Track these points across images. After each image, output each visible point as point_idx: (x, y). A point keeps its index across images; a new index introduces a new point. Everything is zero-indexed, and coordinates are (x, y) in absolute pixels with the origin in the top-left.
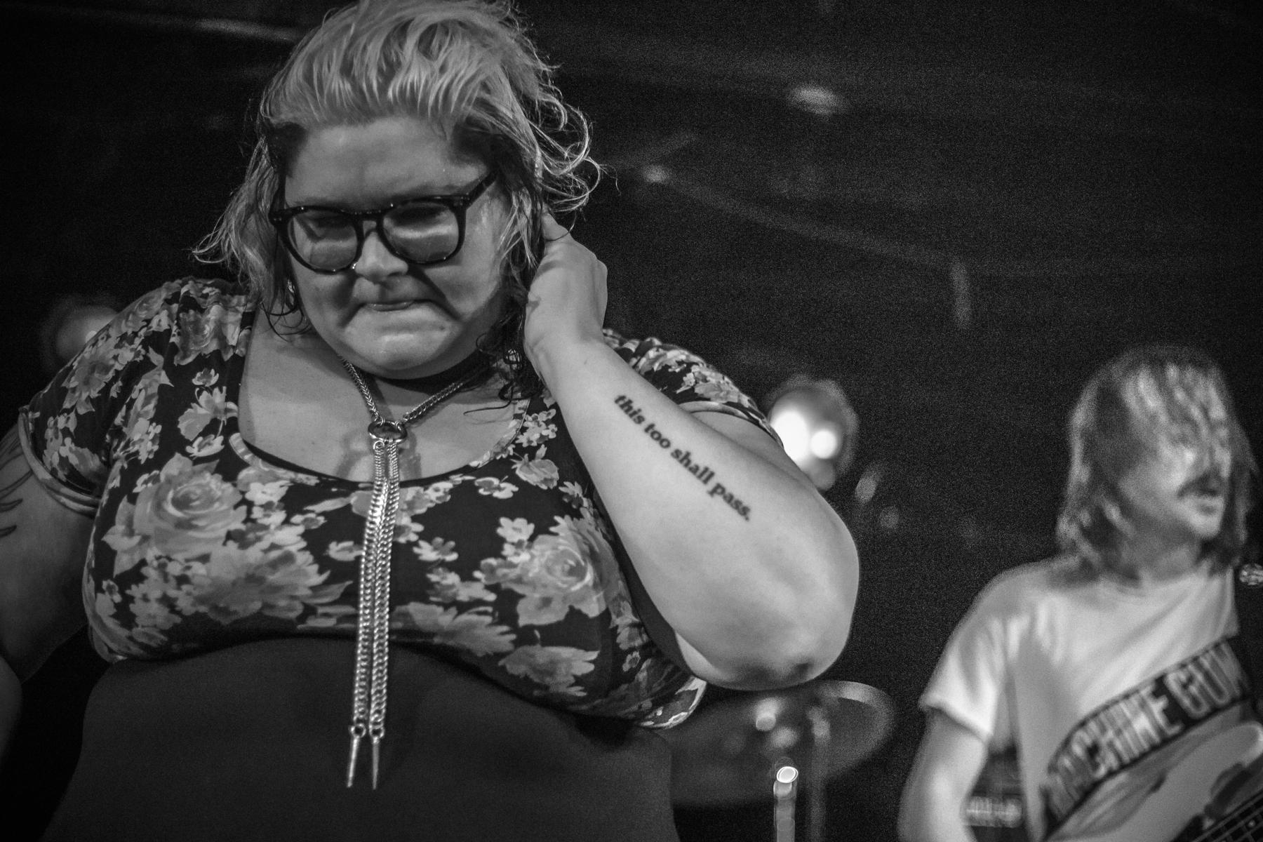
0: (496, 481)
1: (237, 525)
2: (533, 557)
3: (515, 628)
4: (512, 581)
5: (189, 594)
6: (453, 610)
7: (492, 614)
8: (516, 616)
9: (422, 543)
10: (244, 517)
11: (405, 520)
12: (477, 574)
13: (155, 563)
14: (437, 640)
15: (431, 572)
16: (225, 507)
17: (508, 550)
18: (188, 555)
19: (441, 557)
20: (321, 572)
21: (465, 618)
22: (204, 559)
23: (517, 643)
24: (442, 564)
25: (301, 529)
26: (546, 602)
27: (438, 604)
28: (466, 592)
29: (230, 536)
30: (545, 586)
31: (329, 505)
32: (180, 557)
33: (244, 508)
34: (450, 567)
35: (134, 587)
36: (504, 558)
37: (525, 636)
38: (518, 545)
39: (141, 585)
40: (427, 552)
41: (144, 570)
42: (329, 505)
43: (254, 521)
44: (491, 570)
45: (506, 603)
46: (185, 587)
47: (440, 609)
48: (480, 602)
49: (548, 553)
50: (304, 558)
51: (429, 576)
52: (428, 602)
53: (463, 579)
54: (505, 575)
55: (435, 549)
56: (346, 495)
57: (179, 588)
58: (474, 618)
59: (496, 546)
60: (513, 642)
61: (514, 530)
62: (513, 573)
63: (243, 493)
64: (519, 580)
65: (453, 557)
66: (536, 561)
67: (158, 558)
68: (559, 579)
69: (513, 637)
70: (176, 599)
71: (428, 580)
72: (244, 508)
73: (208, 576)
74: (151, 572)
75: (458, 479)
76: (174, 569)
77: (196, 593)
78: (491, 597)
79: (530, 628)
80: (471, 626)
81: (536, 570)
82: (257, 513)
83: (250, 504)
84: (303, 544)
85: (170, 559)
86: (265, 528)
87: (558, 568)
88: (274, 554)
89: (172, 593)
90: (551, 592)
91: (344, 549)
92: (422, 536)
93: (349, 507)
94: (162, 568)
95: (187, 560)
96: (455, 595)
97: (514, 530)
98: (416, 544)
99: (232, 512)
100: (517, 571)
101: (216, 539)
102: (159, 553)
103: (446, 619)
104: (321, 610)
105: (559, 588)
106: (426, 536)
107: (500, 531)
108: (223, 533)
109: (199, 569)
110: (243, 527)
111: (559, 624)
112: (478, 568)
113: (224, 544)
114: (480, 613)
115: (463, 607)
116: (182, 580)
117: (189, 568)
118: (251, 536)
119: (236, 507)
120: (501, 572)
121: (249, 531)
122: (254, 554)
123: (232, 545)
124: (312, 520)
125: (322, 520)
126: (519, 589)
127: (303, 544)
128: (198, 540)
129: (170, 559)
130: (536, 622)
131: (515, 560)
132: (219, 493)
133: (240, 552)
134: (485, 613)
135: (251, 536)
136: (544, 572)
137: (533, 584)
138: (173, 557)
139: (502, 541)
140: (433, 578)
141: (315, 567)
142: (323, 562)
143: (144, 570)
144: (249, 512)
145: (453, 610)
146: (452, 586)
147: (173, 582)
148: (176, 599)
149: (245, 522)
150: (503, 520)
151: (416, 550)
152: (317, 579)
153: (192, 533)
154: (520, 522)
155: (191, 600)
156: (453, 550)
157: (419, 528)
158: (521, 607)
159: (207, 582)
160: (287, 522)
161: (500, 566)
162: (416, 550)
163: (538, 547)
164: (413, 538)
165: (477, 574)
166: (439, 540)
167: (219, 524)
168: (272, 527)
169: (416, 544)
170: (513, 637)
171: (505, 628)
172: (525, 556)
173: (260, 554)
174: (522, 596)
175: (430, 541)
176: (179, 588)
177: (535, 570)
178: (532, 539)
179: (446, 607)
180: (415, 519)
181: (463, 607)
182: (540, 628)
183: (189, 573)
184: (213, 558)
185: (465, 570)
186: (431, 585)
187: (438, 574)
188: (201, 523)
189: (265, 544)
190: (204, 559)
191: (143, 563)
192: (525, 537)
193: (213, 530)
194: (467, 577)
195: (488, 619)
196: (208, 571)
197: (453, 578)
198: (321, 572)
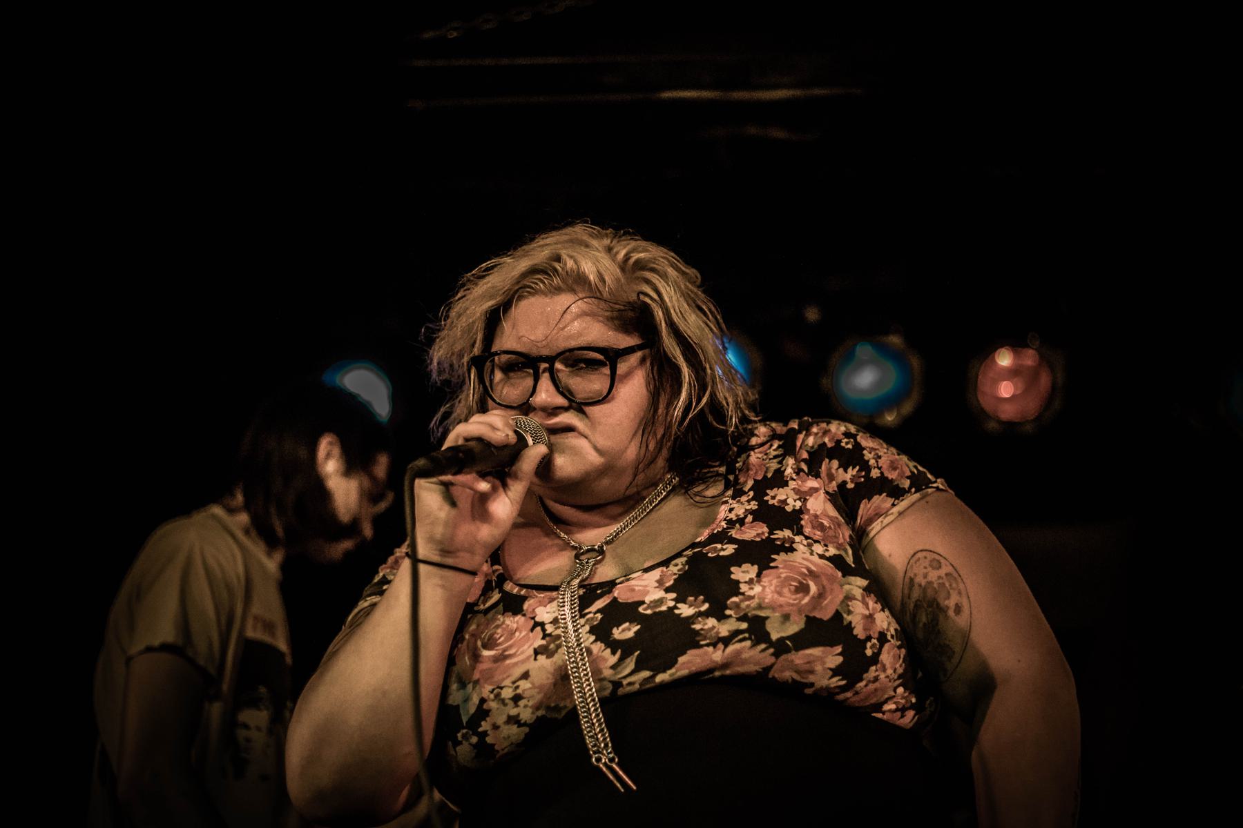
0: (719, 546)
1: (539, 642)
2: (764, 587)
3: (771, 644)
4: (754, 609)
5: (526, 706)
6: (721, 646)
7: (750, 638)
8: (768, 634)
9: (679, 605)
11: (660, 594)
12: (728, 612)
13: (492, 696)
14: (717, 674)
16: (524, 633)
17: (744, 588)
18: (513, 678)
20: (614, 653)
21: (731, 648)
22: (526, 676)
23: (777, 655)
24: (700, 614)
25: (587, 628)
26: (786, 617)
27: (708, 645)
28: (724, 630)
30: (781, 606)
31: (600, 604)
32: (507, 682)
33: (539, 628)
34: (706, 614)
36: (743, 594)
37: (780, 647)
38: (751, 582)
40: (685, 610)
42: (600, 604)
43: (550, 635)
44: (737, 606)
45: (756, 628)
47: (711, 649)
48: (737, 632)
49: (775, 581)
50: (597, 648)
52: (702, 646)
53: (719, 620)
54: (748, 606)
56: (610, 592)
57: (517, 706)
58: (737, 646)
59: (734, 588)
60: (773, 654)
61: (743, 573)
62: (754, 603)
63: (533, 618)
64: (760, 607)
65: (706, 606)
66: (767, 590)
67: (492, 692)
68: (788, 598)
69: (772, 650)
72: (539, 628)
73: (534, 687)
75: (689, 553)
76: (507, 693)
77: (530, 704)
78: (744, 626)
79: (781, 640)
80: (738, 653)
81: (769, 596)
82: (549, 629)
83: (542, 625)
84: (593, 638)
85: (501, 688)
87: (786, 590)
89: (514, 712)
90: (787, 609)
91: (623, 630)
92: (677, 600)
93: (615, 599)
94: (498, 696)
95: (514, 683)
96: (718, 633)
97: (743, 573)
98: (676, 607)
100: (756, 601)
101: (528, 658)
102: (490, 688)
103: (717, 655)
104: (625, 682)
105: (793, 605)
107: (733, 577)
108: (531, 651)
109: (524, 685)
110: (544, 642)
111: (801, 631)
112: (727, 608)
114: (740, 641)
115: (726, 641)
116: (517, 699)
117: (517, 687)
119: (532, 630)
120: (744, 605)
121: (548, 644)
123: (542, 659)
124: (592, 619)
125: (599, 616)
126: (762, 614)
127: (593, 638)
128: (516, 664)
130: (784, 635)
131: (751, 593)
132: (515, 626)
133: (549, 661)
134: (744, 639)
135: (552, 646)
136: (776, 596)
137: (772, 607)
139: (738, 582)
140: (697, 627)
141: (609, 650)
142: (614, 645)
144: (544, 630)
145: (721, 646)
146: (714, 627)
149: (543, 638)
150: (733, 569)
151: (677, 611)
152: (613, 660)
153: (508, 662)
154: (746, 566)
156: (704, 602)
157: (674, 595)
158: (770, 626)
161: (742, 601)
162: (677, 611)
163: (765, 580)
164: (672, 604)
165: (728, 612)
166: (691, 598)
170: (772, 650)
171: (763, 646)
172: (757, 589)
174: (767, 618)
175: (684, 602)
177: (769, 596)
178: (759, 575)
179: (714, 645)
180: (667, 590)
181: (726, 641)
182: (788, 638)
183: (519, 691)
185: (718, 612)
186: (697, 633)
192: (753, 575)
194: (721, 617)
195: (748, 643)
196: (533, 684)
197: (711, 622)
198: (614, 653)
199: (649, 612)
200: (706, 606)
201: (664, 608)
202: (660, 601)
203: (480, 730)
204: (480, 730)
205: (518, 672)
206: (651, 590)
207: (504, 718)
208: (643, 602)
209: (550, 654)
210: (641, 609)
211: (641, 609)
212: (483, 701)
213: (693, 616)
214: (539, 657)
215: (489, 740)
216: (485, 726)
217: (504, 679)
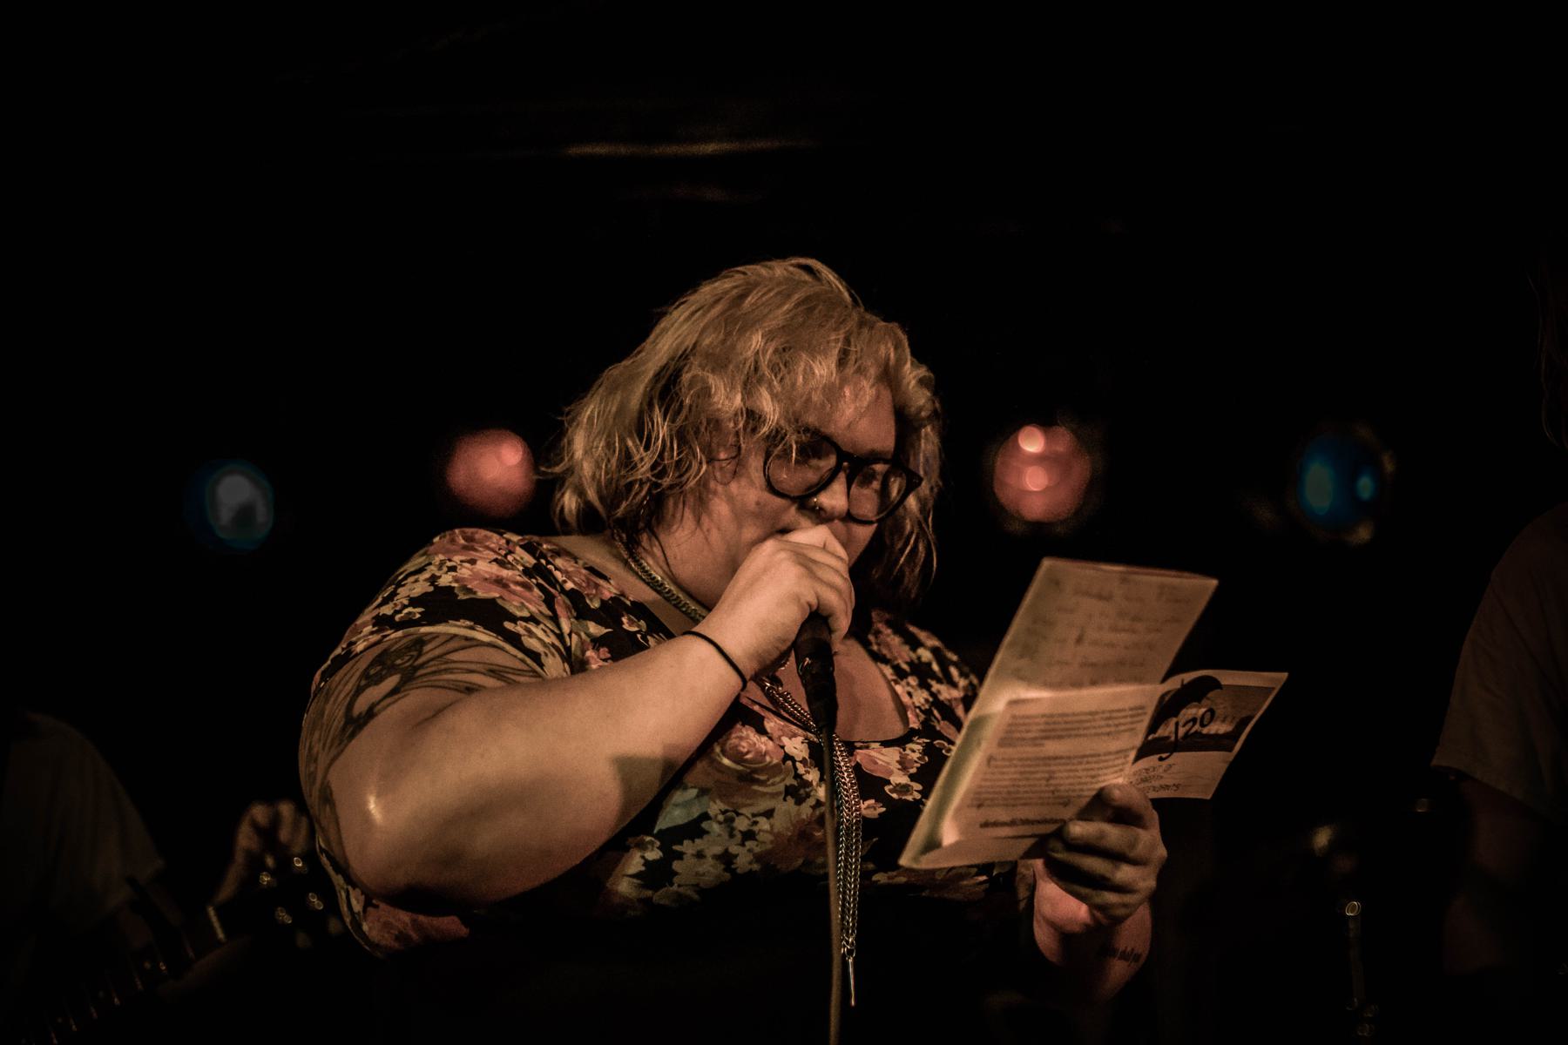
1: (790, 781)
13: (721, 818)
18: (755, 810)
22: (769, 814)
35: (686, 842)
39: (697, 841)
41: (704, 825)
46: (749, 844)
67: (724, 813)
76: (742, 824)
85: (738, 814)
89: (734, 849)
95: (754, 815)
101: (778, 794)
102: (723, 807)
108: (781, 787)
109: (764, 824)
116: (749, 835)
117: (756, 823)
143: (704, 825)
147: (739, 836)
153: (756, 787)
176: (743, 845)
183: (756, 828)
190: (769, 814)
203: (677, 848)
204: (677, 848)
205: (764, 805)
207: (718, 850)
212: (705, 816)
215: (677, 865)
216: (688, 847)
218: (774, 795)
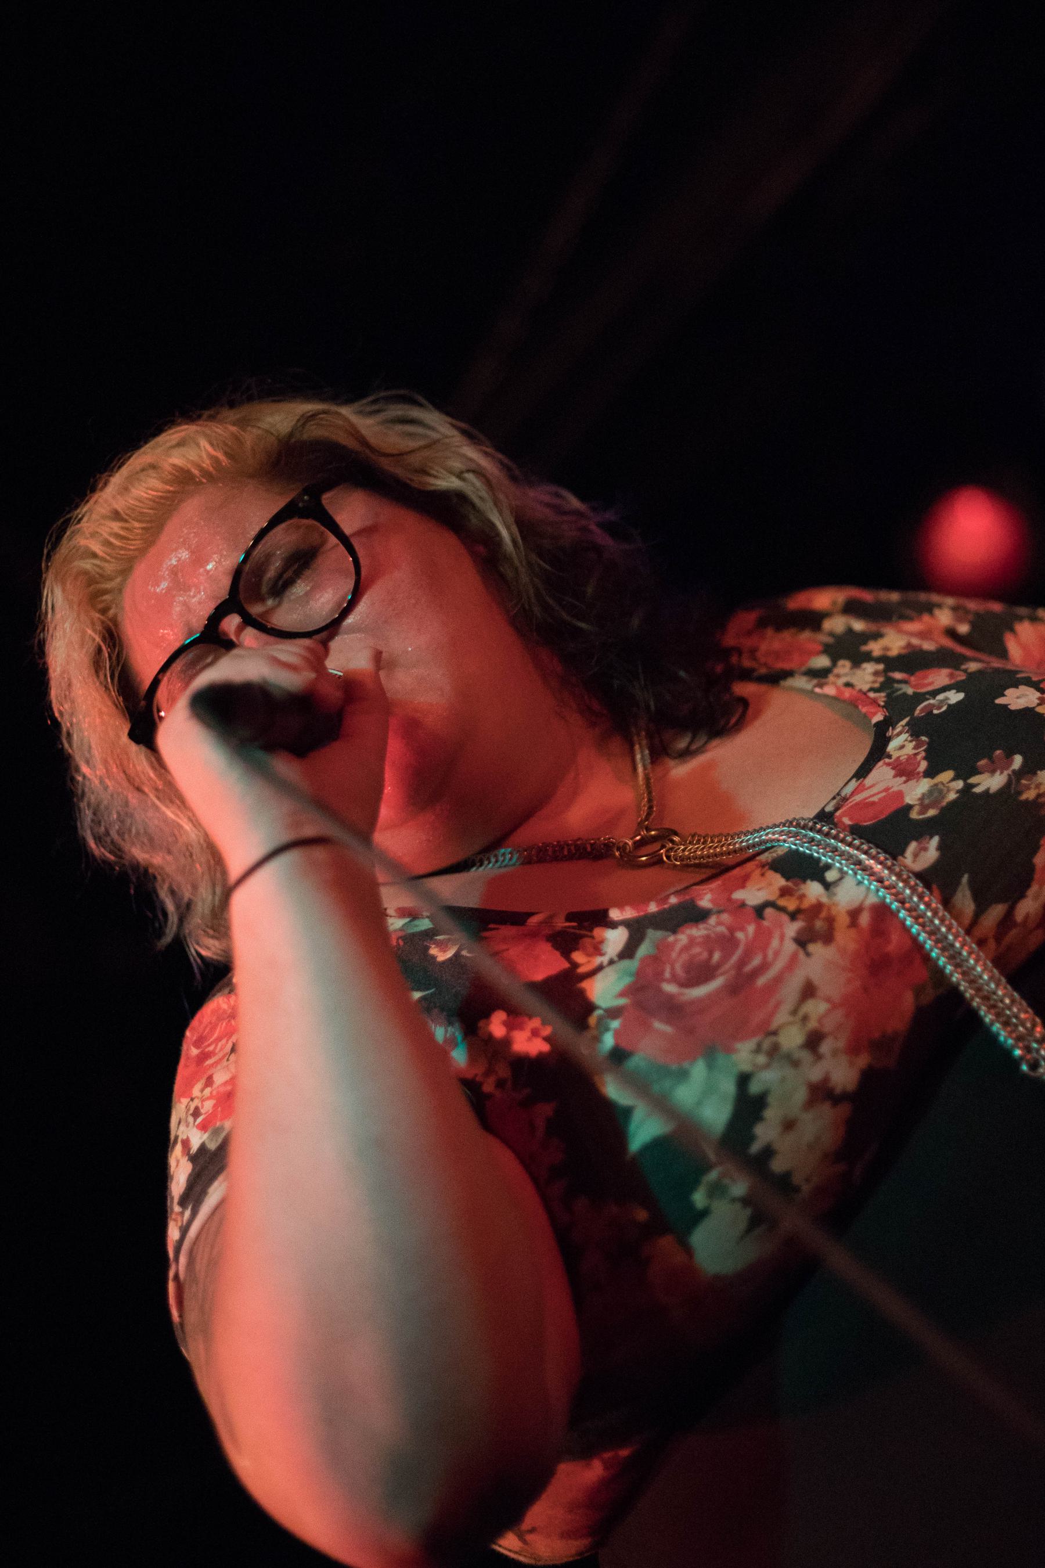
5: (835, 1053)
9: (972, 780)
10: (785, 918)
11: (924, 786)
15: (1020, 793)
16: (751, 929)
19: (1009, 771)
22: (809, 991)
24: (1019, 774)
29: (802, 941)
40: (991, 782)
46: (825, 1048)
51: (1024, 797)
55: (993, 772)
57: (819, 1057)
65: (1018, 761)
70: (826, 1080)
71: (1027, 801)
73: (834, 1007)
74: (766, 1079)
76: (792, 1038)
77: (841, 1044)
85: (775, 1033)
86: (818, 907)
88: (865, 919)
95: (794, 1012)
98: (969, 787)
99: (766, 923)
101: (793, 960)
106: (965, 771)
108: (790, 947)
109: (816, 1008)
113: (808, 954)
116: (813, 1041)
117: (805, 1018)
118: (819, 924)
122: (846, 939)
128: (778, 980)
129: (775, 1033)
138: (774, 1026)
140: (1030, 795)
144: (782, 909)
147: (806, 1056)
148: (826, 1080)
155: (844, 1059)
157: (947, 775)
159: (838, 1015)
160: (827, 886)
162: (977, 790)
164: (960, 784)
166: (983, 762)
167: (775, 943)
168: (824, 900)
169: (969, 787)
173: (853, 933)
175: (976, 772)
176: (819, 1057)
180: (930, 773)
183: (813, 1024)
184: (816, 980)
187: (1028, 788)
188: (756, 961)
189: (843, 920)
190: (809, 991)
191: (743, 1080)
193: (777, 953)
196: (828, 1000)
199: (932, 813)
200: (1018, 761)
201: (952, 796)
202: (936, 793)
206: (904, 788)
208: (910, 807)
209: (828, 938)
210: (914, 815)
211: (914, 815)
213: (1008, 784)
214: (812, 948)
217: (772, 1014)
218: (792, 963)
